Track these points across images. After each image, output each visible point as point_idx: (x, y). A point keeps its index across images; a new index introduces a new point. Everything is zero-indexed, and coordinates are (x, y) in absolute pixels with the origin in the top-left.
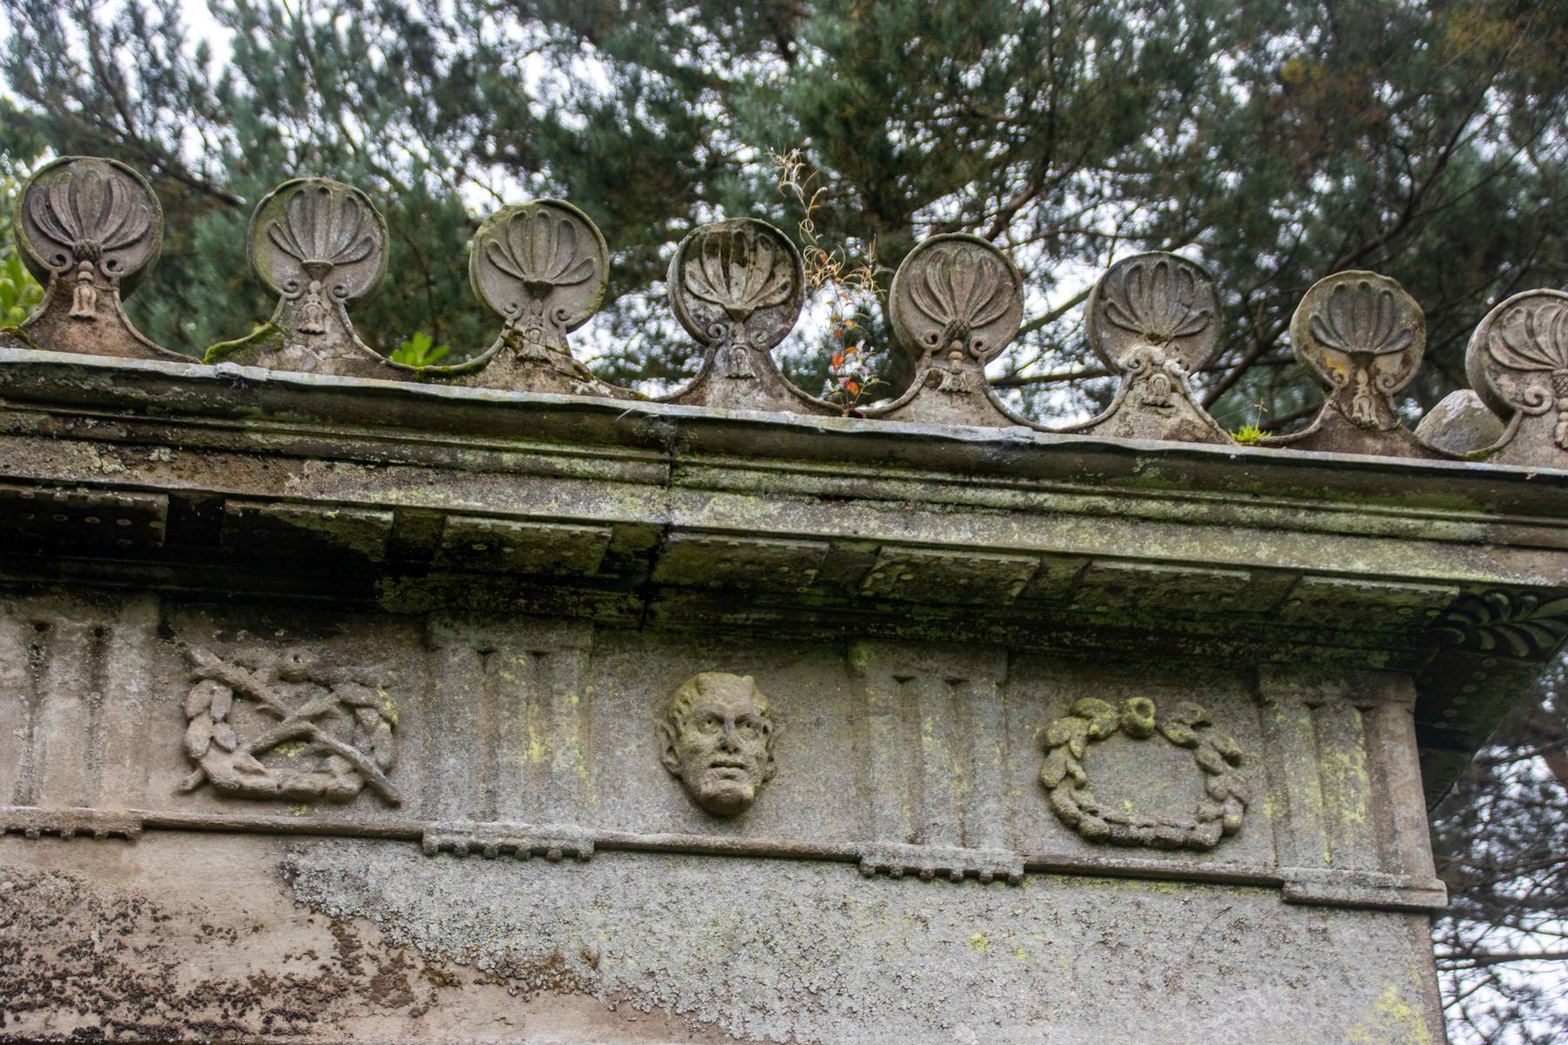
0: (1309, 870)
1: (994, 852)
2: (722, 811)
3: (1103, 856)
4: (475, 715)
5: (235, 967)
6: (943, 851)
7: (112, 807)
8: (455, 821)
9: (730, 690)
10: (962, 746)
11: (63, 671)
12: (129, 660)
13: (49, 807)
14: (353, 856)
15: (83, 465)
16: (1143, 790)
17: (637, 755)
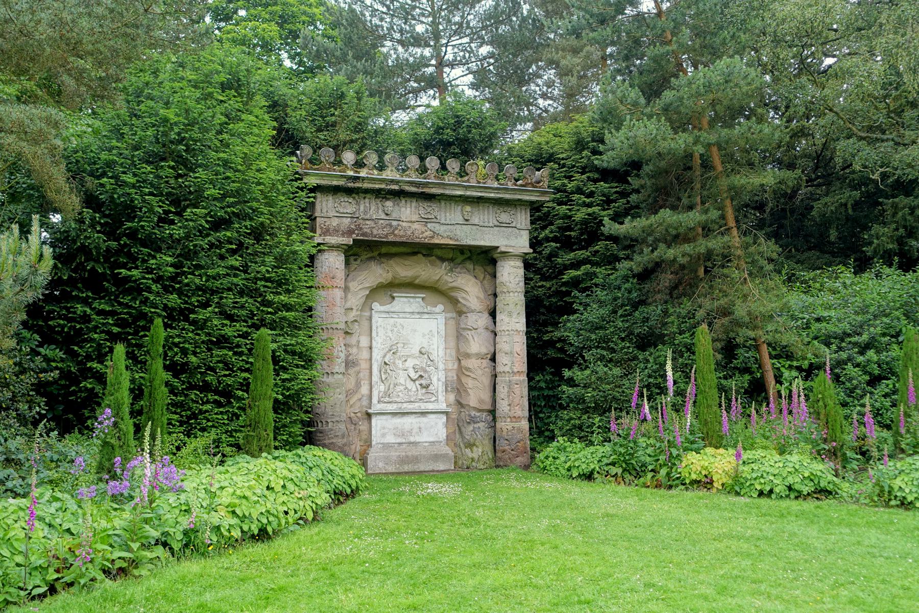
0: (518, 226)
1: (491, 224)
2: (467, 220)
3: (500, 225)
4: (443, 210)
5: (424, 235)
6: (486, 224)
7: (413, 220)
8: (443, 221)
9: (468, 208)
10: (488, 213)
11: (408, 205)
12: (414, 204)
13: (408, 219)
14: (434, 224)
15: (414, 189)
16: (504, 217)
17: (459, 214)
